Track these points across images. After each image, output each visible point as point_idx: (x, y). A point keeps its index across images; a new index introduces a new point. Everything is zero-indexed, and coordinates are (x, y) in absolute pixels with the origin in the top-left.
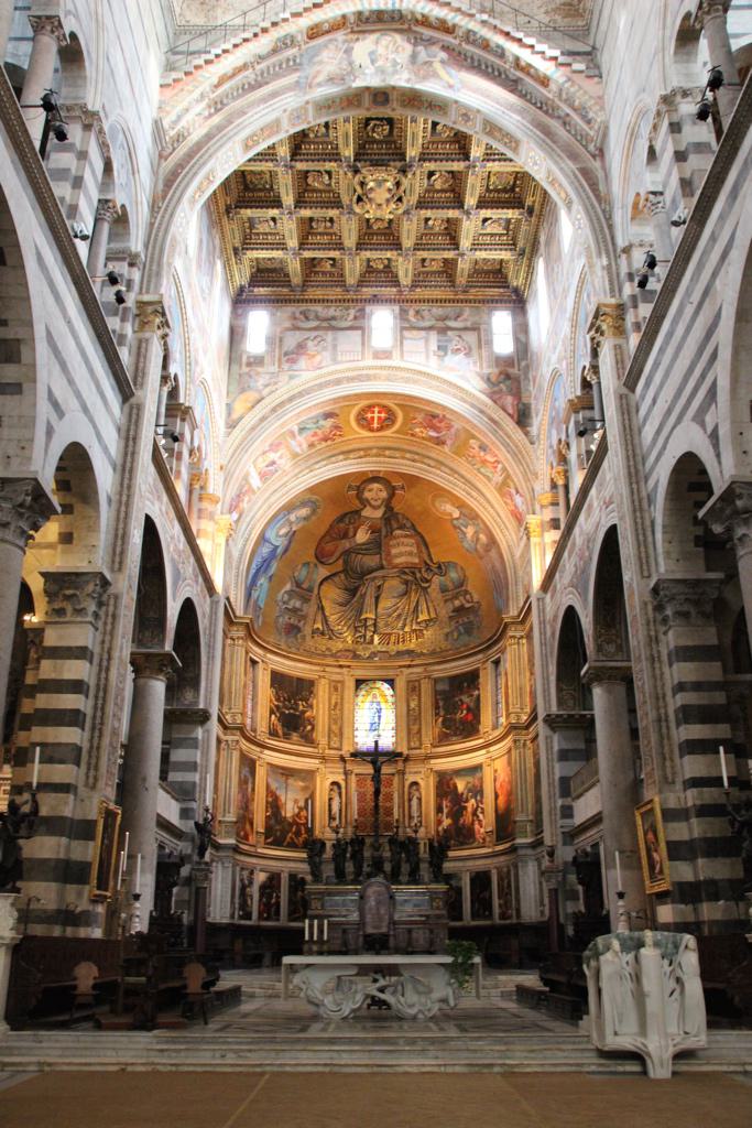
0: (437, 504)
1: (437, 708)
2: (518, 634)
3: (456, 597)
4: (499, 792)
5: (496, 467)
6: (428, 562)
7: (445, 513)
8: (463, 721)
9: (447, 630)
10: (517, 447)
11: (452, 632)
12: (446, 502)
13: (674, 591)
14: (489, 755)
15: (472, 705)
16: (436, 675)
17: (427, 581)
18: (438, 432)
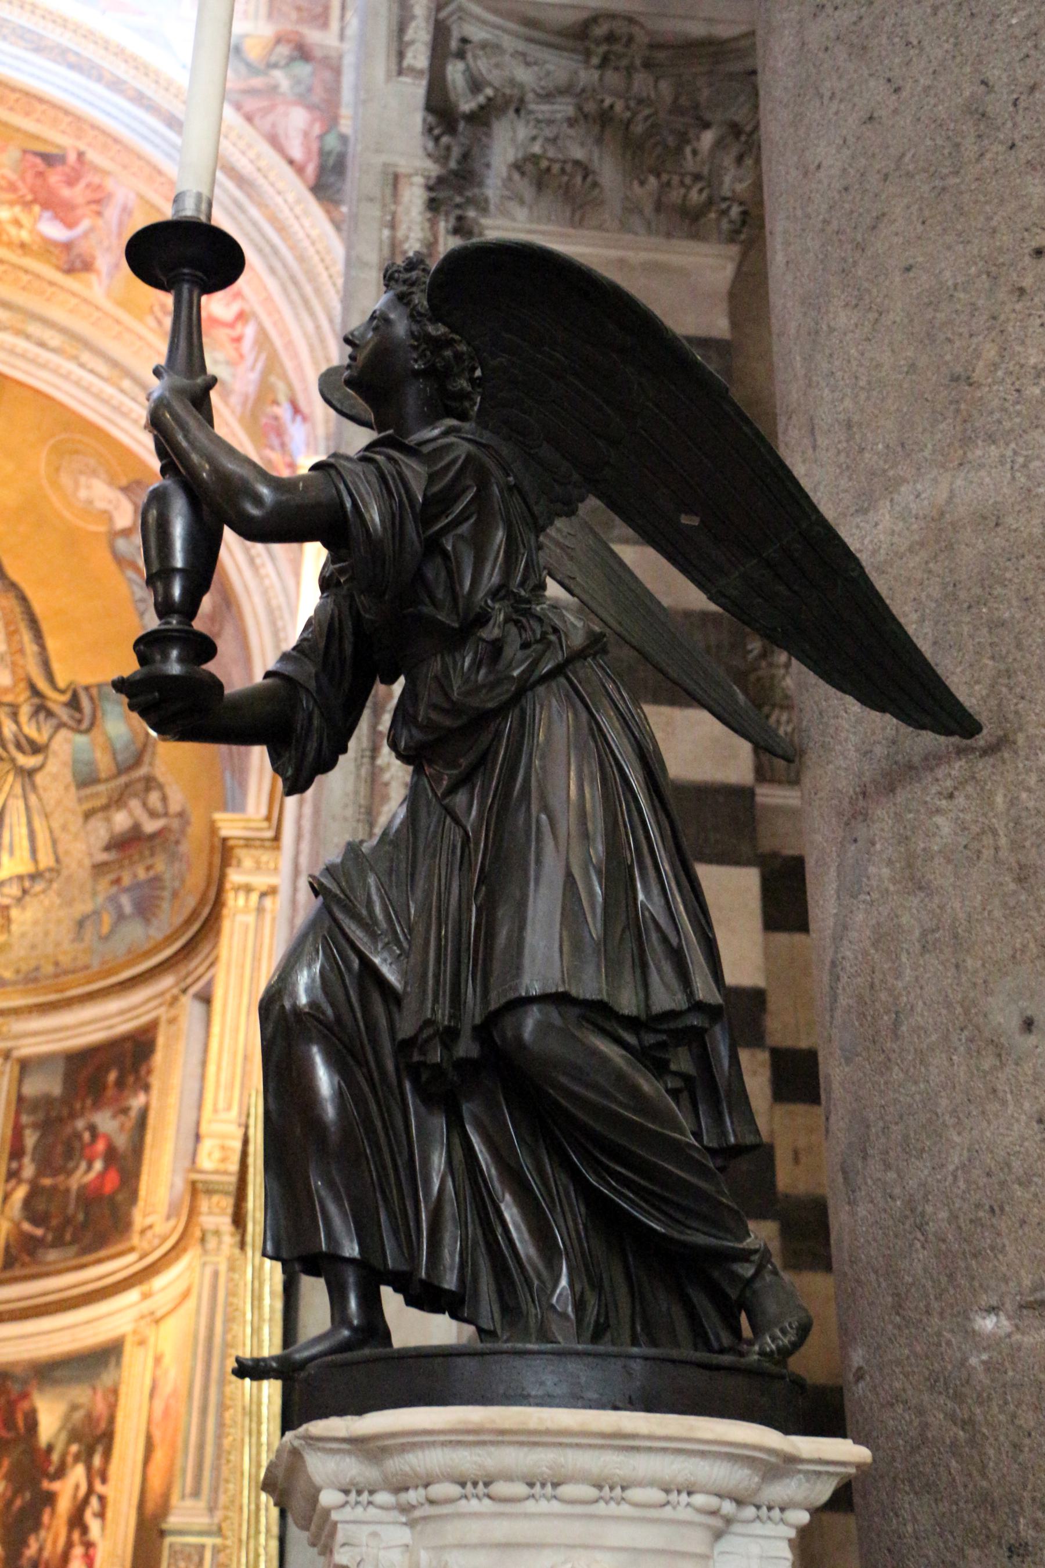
0: (65, 479)
1: (17, 1152)
2: (262, 881)
3: (118, 801)
4: (157, 1435)
5: (238, 340)
6: (42, 685)
7: (88, 510)
8: (90, 1198)
9: (84, 907)
10: (301, 259)
11: (96, 913)
12: (94, 473)
13: (524, 75)
14: (147, 1306)
15: (121, 1141)
16: (28, 1048)
17: (36, 748)
18: (70, 225)
